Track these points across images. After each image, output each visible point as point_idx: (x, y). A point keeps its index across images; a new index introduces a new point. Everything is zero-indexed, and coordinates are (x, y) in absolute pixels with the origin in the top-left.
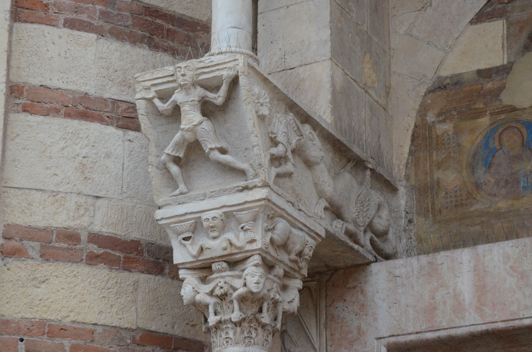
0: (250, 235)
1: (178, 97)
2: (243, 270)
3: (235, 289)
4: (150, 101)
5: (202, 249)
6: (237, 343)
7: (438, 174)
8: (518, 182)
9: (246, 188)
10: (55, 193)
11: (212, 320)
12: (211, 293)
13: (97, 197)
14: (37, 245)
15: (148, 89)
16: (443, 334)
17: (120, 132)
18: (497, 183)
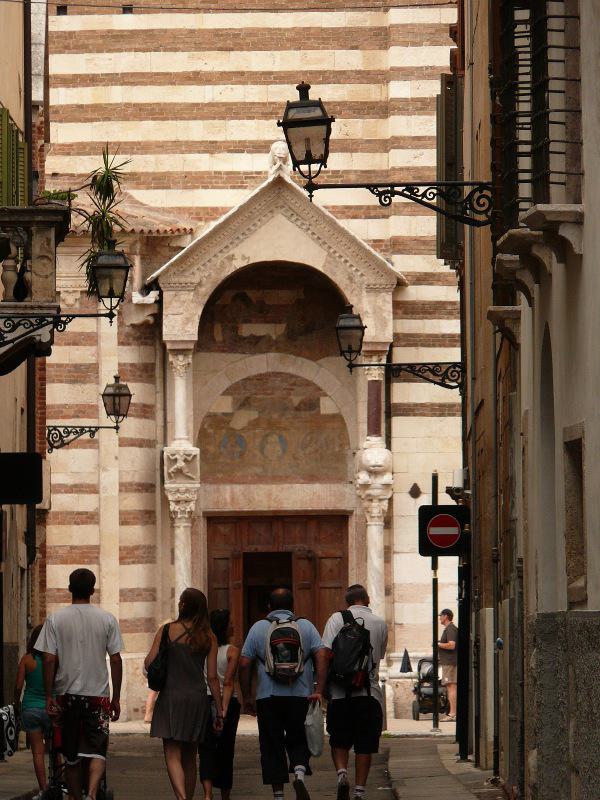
1: (177, 456)
7: (208, 447)
11: (179, 516)
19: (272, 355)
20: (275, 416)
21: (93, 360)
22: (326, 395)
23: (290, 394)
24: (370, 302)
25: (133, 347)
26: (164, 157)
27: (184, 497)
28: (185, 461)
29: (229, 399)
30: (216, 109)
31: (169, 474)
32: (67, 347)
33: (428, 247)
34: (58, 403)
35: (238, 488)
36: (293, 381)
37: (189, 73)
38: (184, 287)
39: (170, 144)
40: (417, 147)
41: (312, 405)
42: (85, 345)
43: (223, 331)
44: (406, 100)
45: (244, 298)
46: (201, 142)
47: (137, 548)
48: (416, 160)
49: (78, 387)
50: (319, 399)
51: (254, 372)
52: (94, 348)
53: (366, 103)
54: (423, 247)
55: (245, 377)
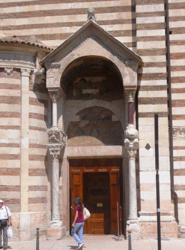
4: (48, 133)
9: (59, 144)
10: (33, 140)
12: (54, 154)
15: (48, 131)
20: (95, 122)
21: (19, 95)
22: (114, 114)
24: (128, 70)
26: (53, 29)
27: (55, 149)
29: (78, 116)
30: (72, 11)
32: (7, 90)
33: (151, 53)
34: (3, 111)
35: (80, 148)
38: (55, 67)
39: (55, 24)
40: (146, 16)
41: (109, 118)
42: (15, 89)
43: (76, 92)
45: (84, 80)
46: (67, 23)
47: (38, 169)
48: (146, 21)
49: (11, 105)
50: (111, 116)
52: (19, 91)
53: (127, 6)
54: (149, 53)
55: (84, 108)
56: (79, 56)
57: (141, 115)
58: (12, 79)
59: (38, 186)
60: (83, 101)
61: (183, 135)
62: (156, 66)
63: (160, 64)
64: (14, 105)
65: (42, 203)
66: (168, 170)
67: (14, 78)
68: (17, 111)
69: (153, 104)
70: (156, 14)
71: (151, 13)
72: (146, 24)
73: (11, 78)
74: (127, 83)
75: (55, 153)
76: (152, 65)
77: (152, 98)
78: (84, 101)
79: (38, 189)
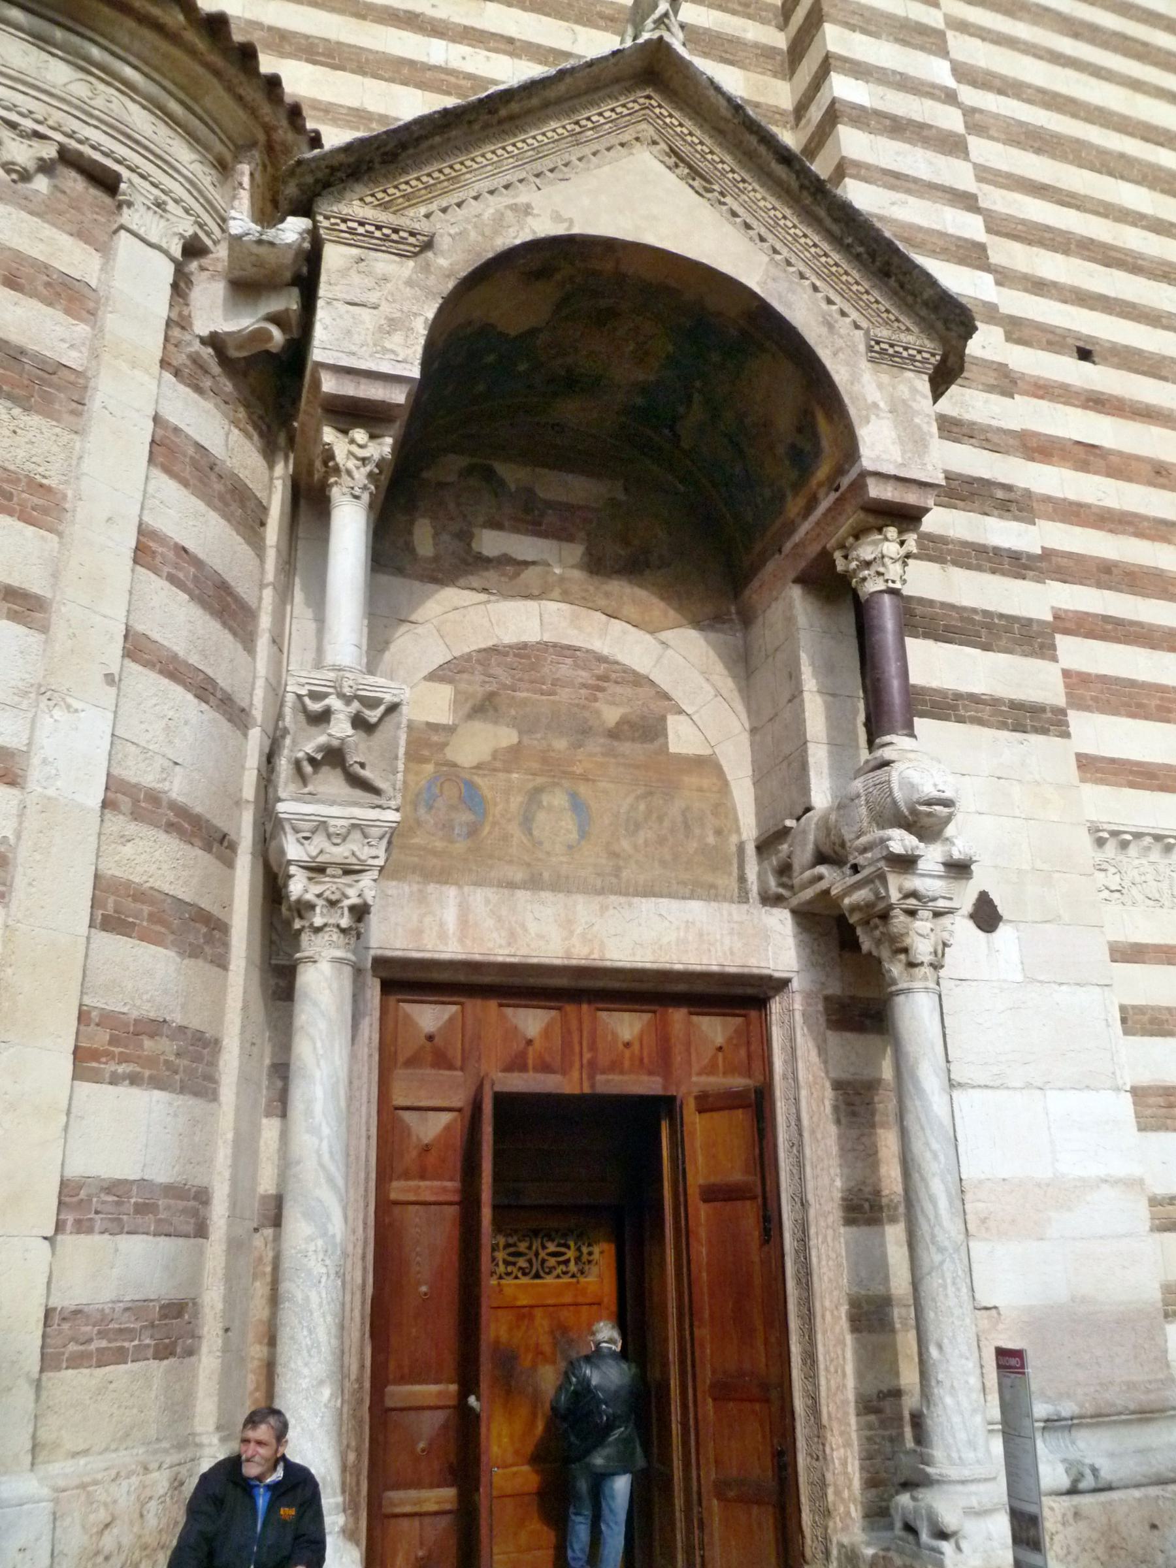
0: (374, 852)
2: (357, 881)
3: (347, 897)
4: (299, 697)
5: (321, 852)
6: (338, 948)
8: (453, 829)
10: (145, 750)
12: (319, 896)
13: (176, 763)
14: (127, 799)
16: (427, 955)
17: (196, 701)
18: (436, 824)
19: (552, 607)
20: (561, 744)
22: (681, 712)
23: (596, 700)
24: (880, 386)
25: (208, 405)
27: (339, 853)
28: (359, 722)
29: (444, 693)
30: (452, 80)
31: (297, 764)
36: (602, 669)
37: (398, 10)
39: (344, 111)
40: (892, 188)
43: (436, 535)
44: (862, 108)
45: (489, 474)
47: (154, 1027)
48: (895, 208)
50: (663, 719)
51: (509, 638)
55: (483, 646)
56: (566, 225)
57: (924, 702)
58: (35, 219)
59: (143, 1184)
60: (483, 597)
61: (1109, 874)
62: (973, 441)
63: (995, 438)
64: (17, 411)
65: (161, 1359)
66: (1120, 1082)
67: (48, 222)
68: (40, 470)
69: (986, 647)
70: (939, 194)
71: (916, 180)
72: (896, 220)
73: (31, 213)
74: (884, 456)
75: (328, 886)
76: (955, 429)
77: (974, 611)
78: (489, 602)
79: (139, 1219)
